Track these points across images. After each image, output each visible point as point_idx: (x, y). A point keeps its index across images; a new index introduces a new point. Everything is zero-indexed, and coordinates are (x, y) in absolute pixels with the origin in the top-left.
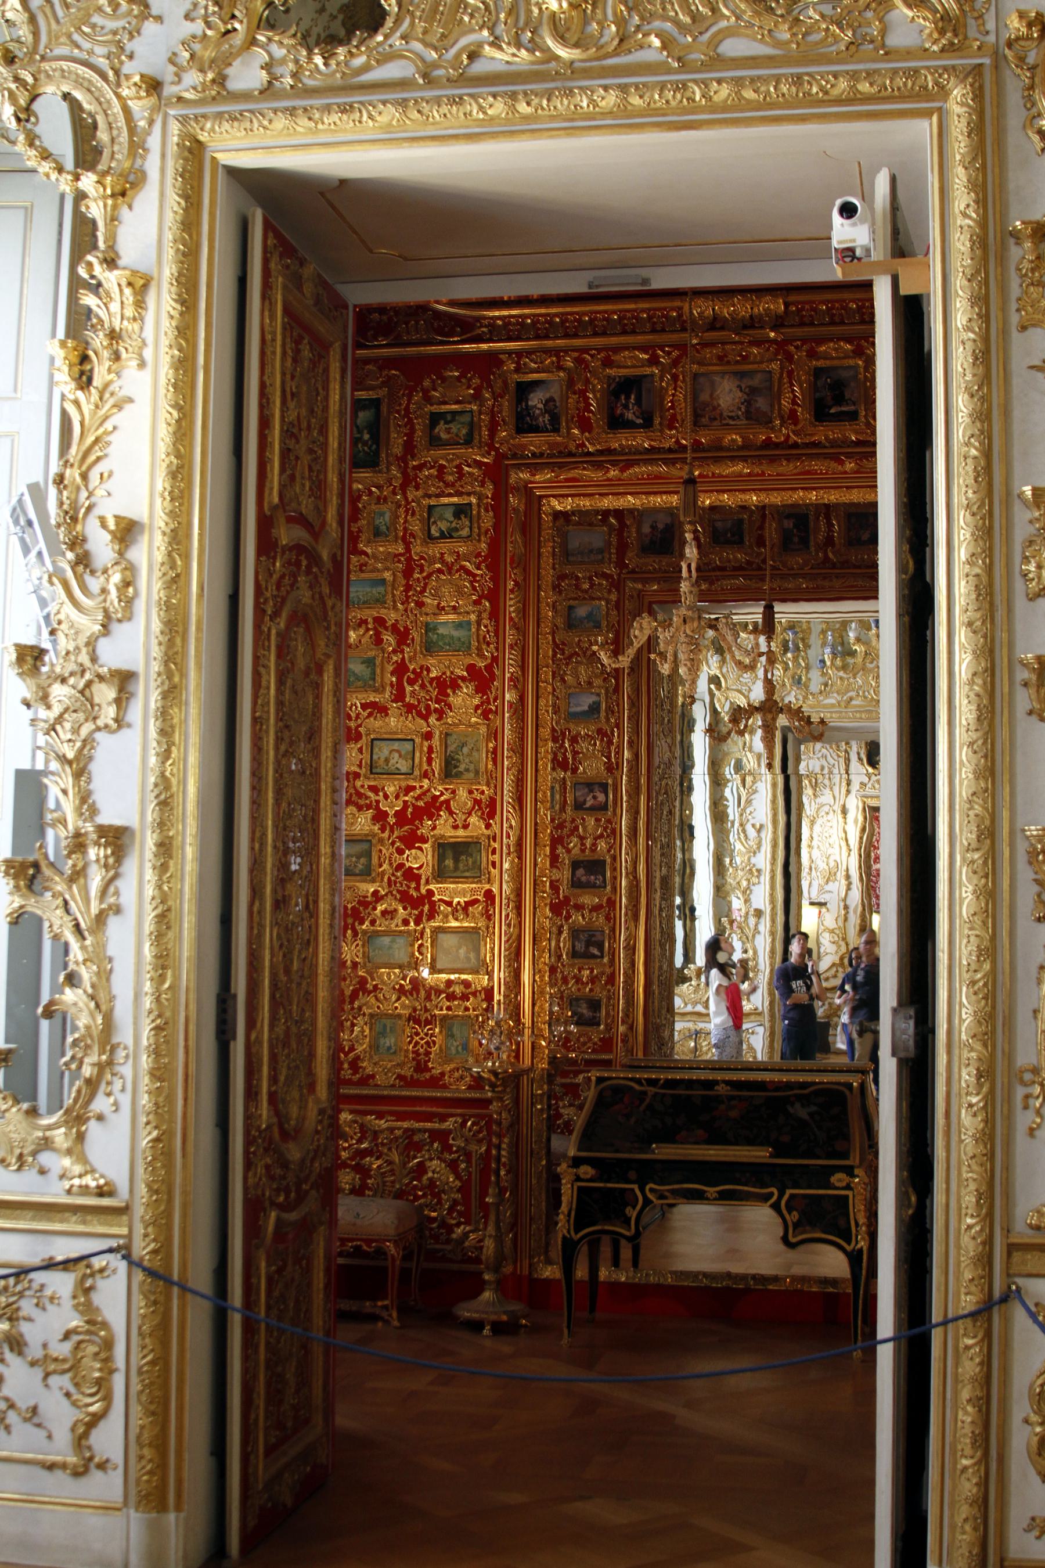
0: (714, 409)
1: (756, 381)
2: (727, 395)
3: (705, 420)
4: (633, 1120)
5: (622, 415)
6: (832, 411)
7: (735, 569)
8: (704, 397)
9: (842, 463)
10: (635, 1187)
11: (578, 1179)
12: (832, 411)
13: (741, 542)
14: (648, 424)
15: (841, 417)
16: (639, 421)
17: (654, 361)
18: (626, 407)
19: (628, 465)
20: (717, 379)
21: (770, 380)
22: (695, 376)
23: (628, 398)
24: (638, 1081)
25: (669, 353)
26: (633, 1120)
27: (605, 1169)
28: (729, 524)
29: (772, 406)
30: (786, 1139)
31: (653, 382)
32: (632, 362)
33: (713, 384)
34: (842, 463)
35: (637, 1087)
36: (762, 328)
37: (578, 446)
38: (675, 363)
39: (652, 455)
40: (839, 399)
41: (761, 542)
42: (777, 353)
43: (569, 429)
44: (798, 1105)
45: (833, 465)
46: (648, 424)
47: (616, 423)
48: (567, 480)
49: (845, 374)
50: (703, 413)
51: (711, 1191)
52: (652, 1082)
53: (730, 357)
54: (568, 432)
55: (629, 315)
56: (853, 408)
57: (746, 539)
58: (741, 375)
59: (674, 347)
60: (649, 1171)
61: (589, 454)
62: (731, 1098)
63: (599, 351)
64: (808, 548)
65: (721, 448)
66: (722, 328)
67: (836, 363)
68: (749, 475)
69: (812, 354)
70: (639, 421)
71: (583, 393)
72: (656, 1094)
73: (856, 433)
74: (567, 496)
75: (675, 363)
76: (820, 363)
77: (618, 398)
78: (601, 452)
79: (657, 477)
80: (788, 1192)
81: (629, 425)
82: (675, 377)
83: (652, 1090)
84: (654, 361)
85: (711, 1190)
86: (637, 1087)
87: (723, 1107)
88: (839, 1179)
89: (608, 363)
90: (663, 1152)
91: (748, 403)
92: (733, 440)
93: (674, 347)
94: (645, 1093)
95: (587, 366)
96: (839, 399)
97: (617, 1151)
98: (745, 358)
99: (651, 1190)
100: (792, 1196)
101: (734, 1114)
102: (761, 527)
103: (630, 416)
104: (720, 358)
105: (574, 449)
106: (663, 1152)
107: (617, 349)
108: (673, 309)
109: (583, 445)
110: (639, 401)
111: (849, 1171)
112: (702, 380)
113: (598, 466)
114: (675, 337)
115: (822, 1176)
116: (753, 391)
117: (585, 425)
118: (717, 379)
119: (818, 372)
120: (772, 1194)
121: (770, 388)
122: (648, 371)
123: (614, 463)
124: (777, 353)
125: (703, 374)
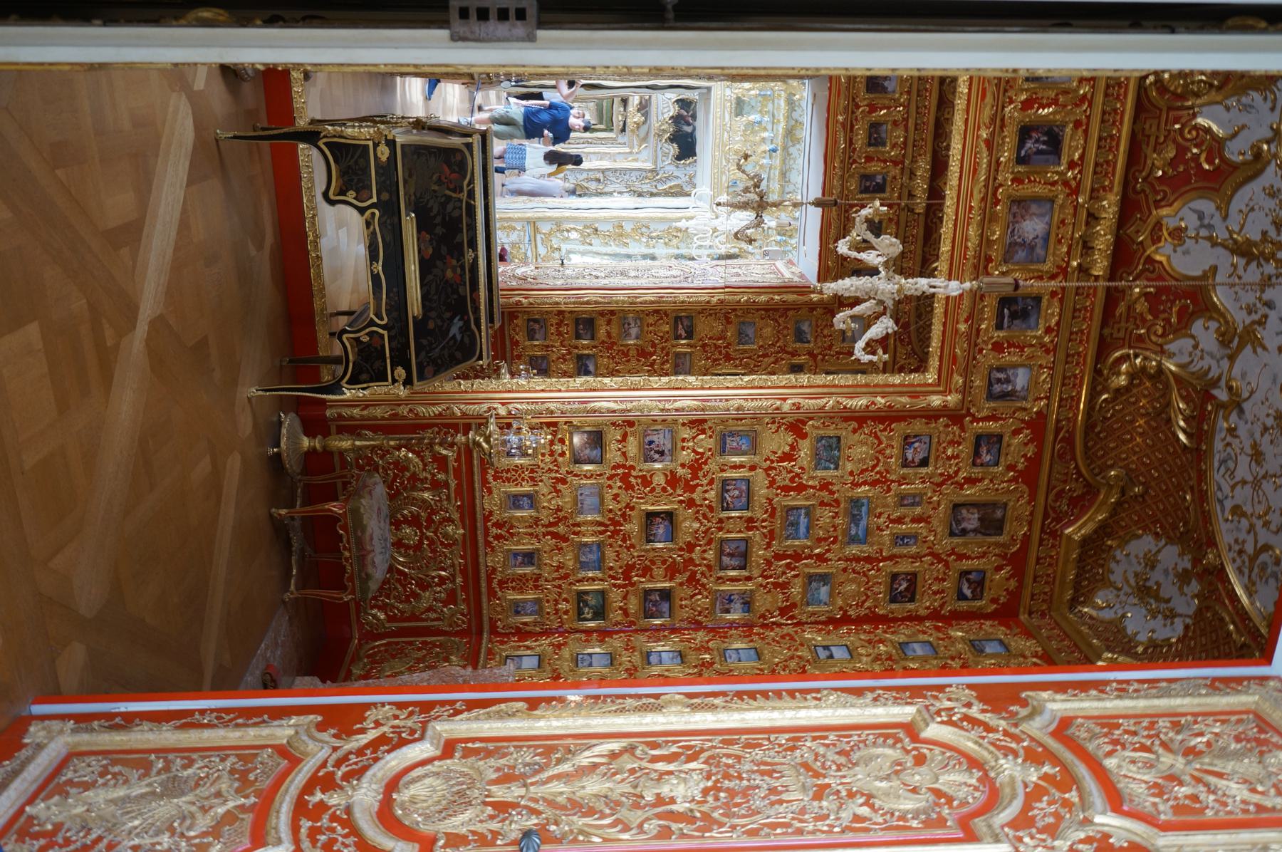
0: (1022, 217)
1: (1039, 251)
2: (1032, 227)
3: (1015, 208)
4: (436, 188)
5: (1030, 137)
6: (1006, 311)
7: (851, 140)
8: (1034, 208)
9: (966, 321)
10: (374, 200)
11: (376, 145)
12: (1006, 311)
13: (870, 145)
14: (1020, 160)
15: (1000, 317)
16: (1023, 153)
17: (1072, 165)
18: (1037, 141)
19: (989, 143)
20: (1047, 218)
21: (1038, 262)
22: (1052, 201)
23: (1044, 143)
24: (472, 181)
25: (1075, 178)
26: (436, 188)
27: (386, 170)
28: (883, 135)
29: (1017, 263)
30: (431, 325)
31: (1054, 164)
32: (1073, 146)
33: (1042, 215)
34: (966, 321)
35: (466, 183)
36: (1082, 255)
37: (1010, 98)
38: (1066, 183)
39: (995, 165)
40: (1013, 316)
41: (869, 159)
42: (1058, 267)
43: (1026, 90)
44: (461, 323)
45: (965, 315)
46: (1020, 160)
47: (1025, 132)
48: (984, 90)
49: (1032, 320)
50: (1020, 205)
51: (379, 268)
52: (471, 194)
53: (1061, 231)
54: (1022, 90)
55: (1114, 144)
56: (1006, 325)
57: (872, 149)
58: (1046, 239)
59: (1079, 184)
60: (389, 210)
61: (1003, 107)
62: (462, 267)
63: (1088, 117)
64: (861, 192)
65: (990, 221)
66: (1087, 223)
67: (1043, 313)
68: (966, 247)
69: (1053, 294)
70: (1023, 153)
71: (1055, 102)
72: (461, 201)
73: (987, 329)
74: (970, 89)
75: (1066, 183)
76: (1045, 302)
77: (1045, 134)
78: (1003, 119)
79: (975, 170)
80: (385, 333)
81: (1021, 143)
82: (1054, 184)
83: (464, 196)
84: (1072, 165)
85: (380, 268)
86: (466, 183)
87: (454, 262)
88: (400, 372)
89: (1077, 124)
90: (409, 224)
91: (1023, 244)
92: (994, 233)
93: (1079, 184)
94: (461, 191)
95: (1077, 105)
96: (1013, 316)
97: (405, 182)
98: (1059, 241)
99: (373, 214)
100: (382, 336)
101: (449, 274)
102: (879, 160)
103: (1029, 145)
104: (1063, 222)
105: (1009, 94)
106: (409, 224)
107: (1086, 132)
108: (1112, 182)
109: (1011, 102)
110: (1039, 152)
111: (408, 382)
112: (1048, 206)
113: (993, 119)
114: (1088, 184)
115: (401, 358)
116: (1032, 248)
117: (1027, 105)
118: (1047, 218)
119: (1038, 299)
120: (382, 319)
121: (1032, 262)
122: (1064, 160)
123: (993, 134)
124: (1058, 267)
125: (1052, 207)
